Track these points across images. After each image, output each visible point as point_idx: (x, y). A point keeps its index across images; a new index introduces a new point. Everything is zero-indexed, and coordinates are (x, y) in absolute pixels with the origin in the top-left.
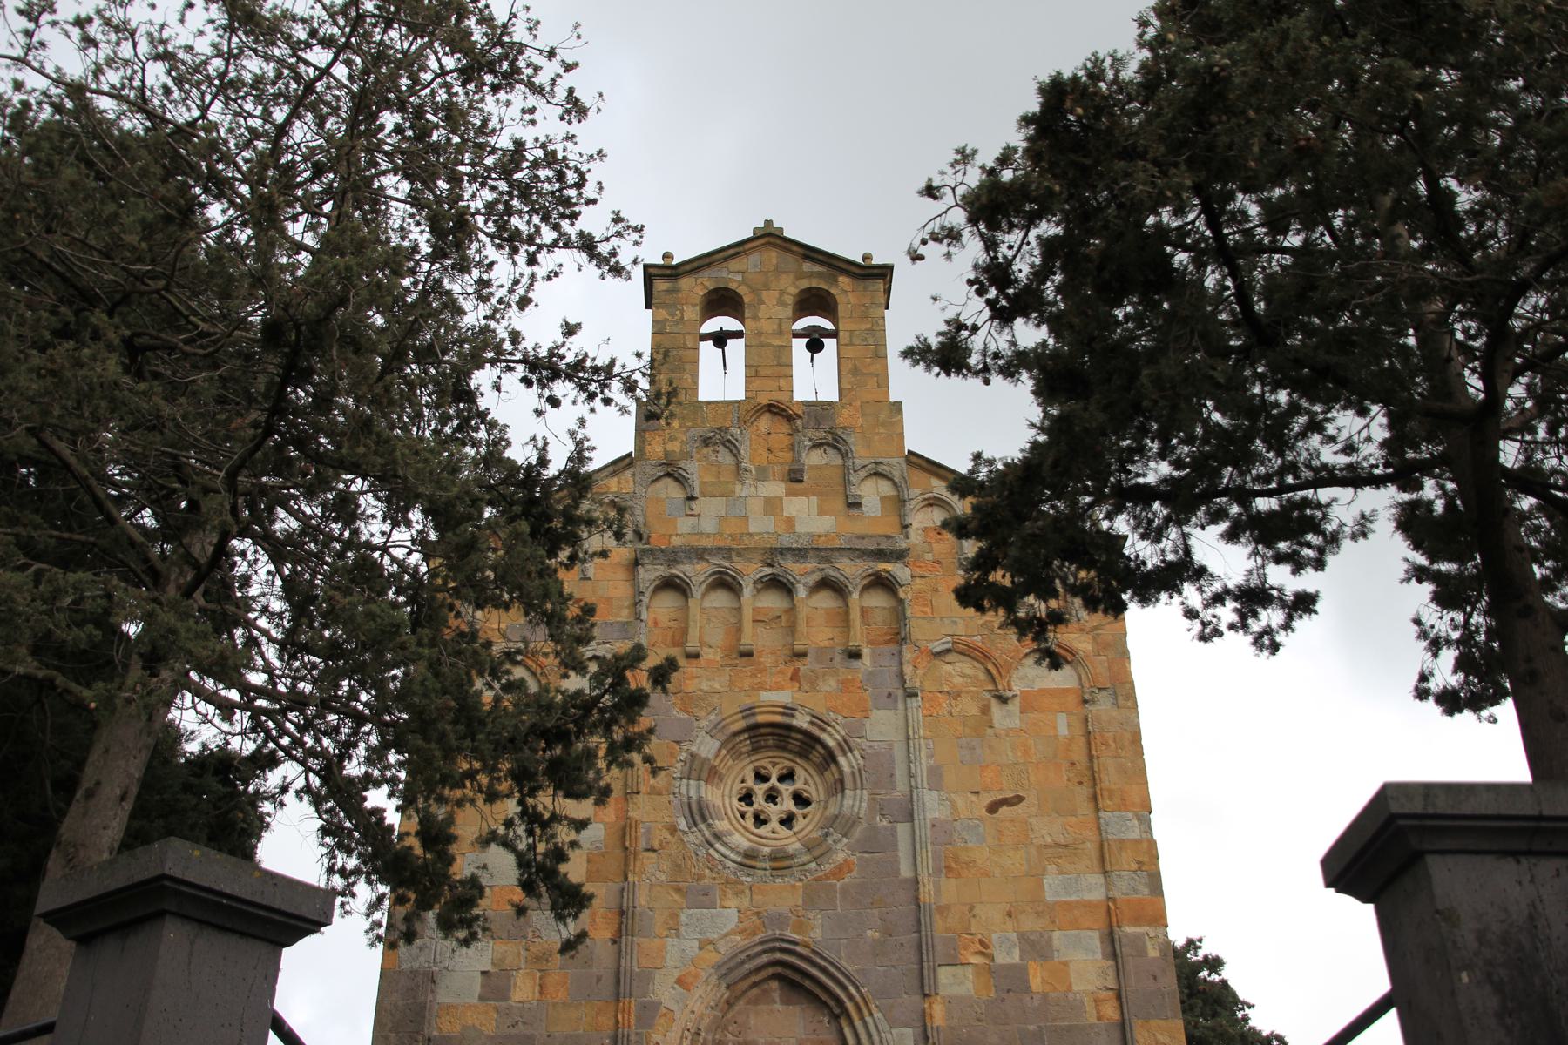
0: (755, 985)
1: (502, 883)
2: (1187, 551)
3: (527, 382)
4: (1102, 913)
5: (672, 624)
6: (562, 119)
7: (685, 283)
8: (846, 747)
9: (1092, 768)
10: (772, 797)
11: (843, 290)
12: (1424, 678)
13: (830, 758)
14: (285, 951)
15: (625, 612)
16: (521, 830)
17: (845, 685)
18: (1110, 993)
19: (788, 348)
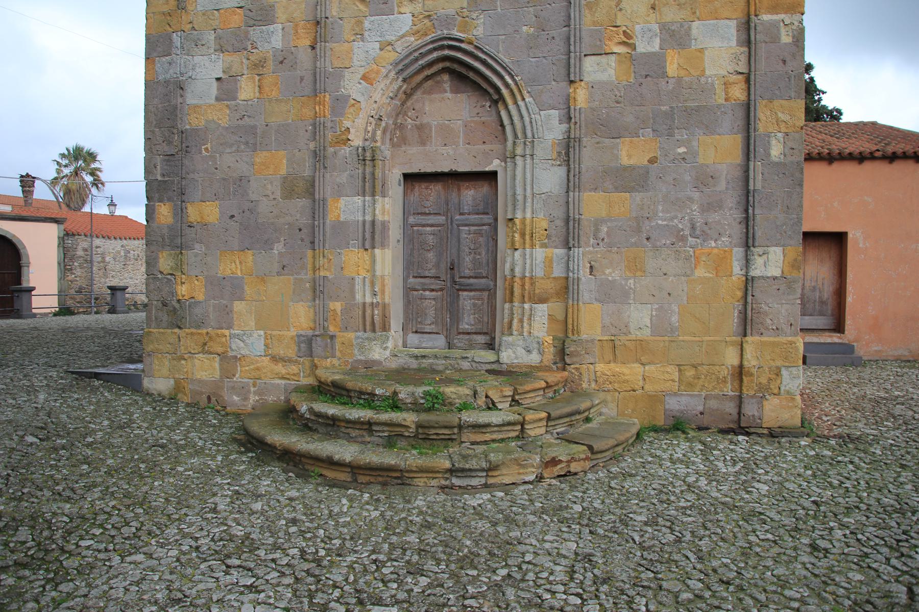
0: (428, 78)
1: (226, 6)
18: (740, 77)
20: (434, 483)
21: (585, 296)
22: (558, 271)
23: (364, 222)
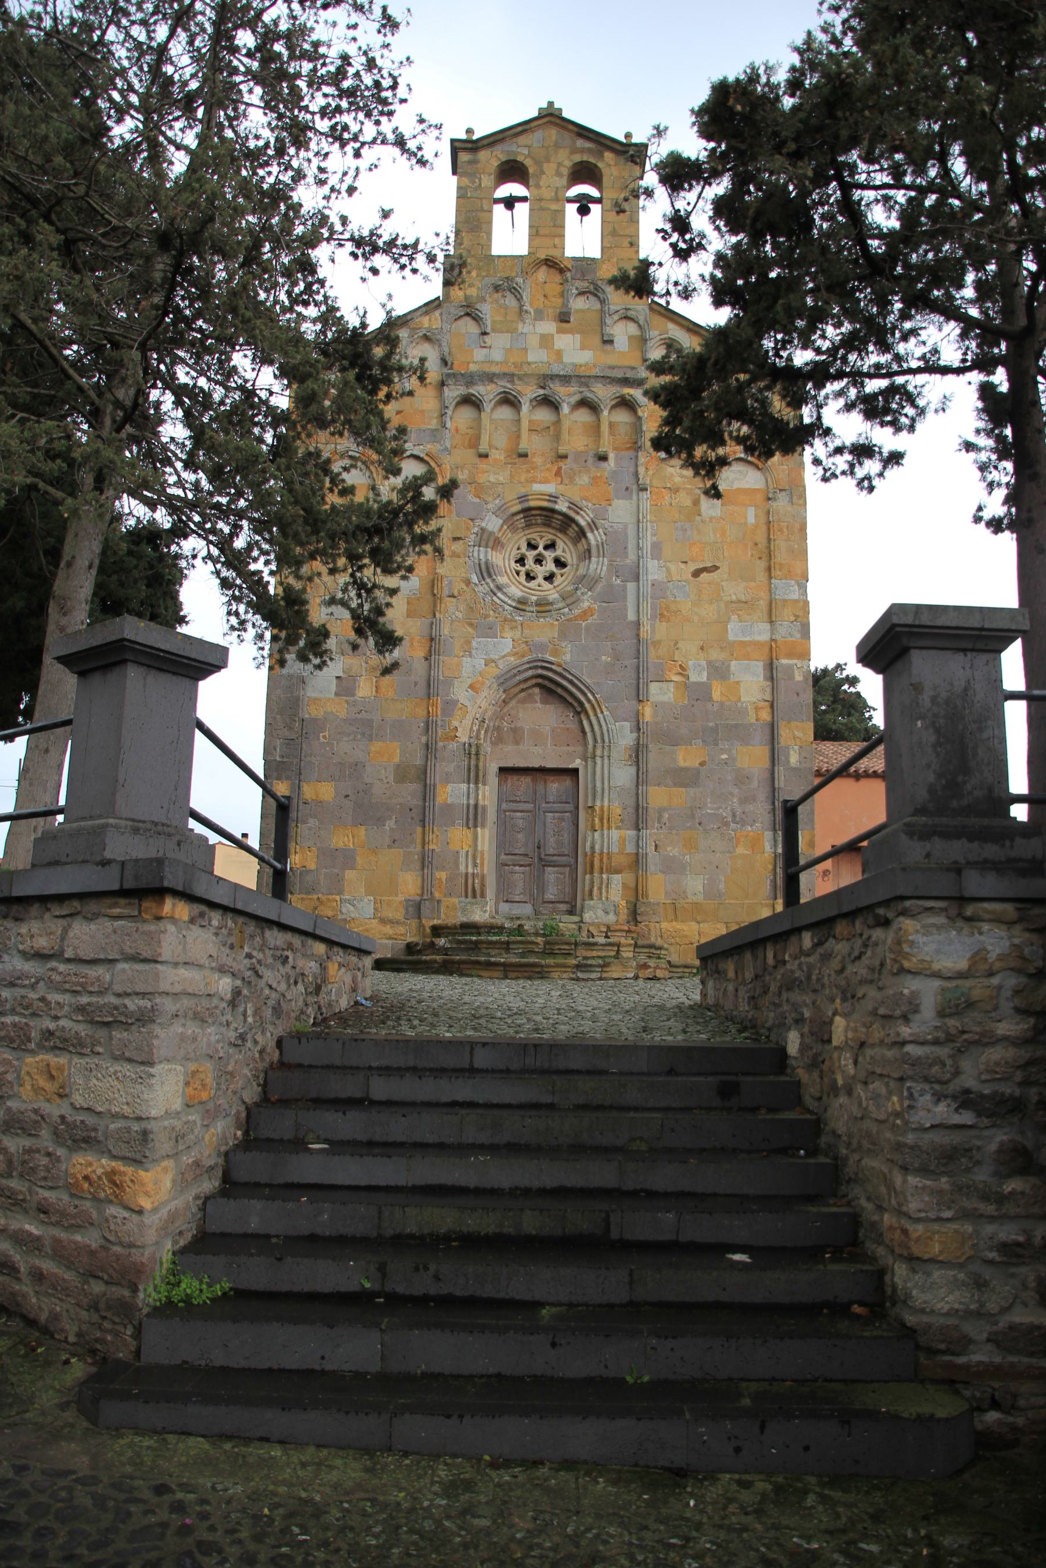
0: (523, 690)
2: (819, 418)
3: (354, 256)
4: (767, 649)
5: (470, 431)
6: (379, 32)
7: (483, 155)
8: (593, 525)
9: (769, 548)
10: (539, 561)
11: (608, 164)
12: (980, 509)
13: (582, 534)
14: (201, 683)
15: (435, 421)
16: (353, 593)
17: (595, 479)
19: (562, 212)
20: (565, 976)
21: (652, 868)
22: (630, 849)
23: (468, 805)
